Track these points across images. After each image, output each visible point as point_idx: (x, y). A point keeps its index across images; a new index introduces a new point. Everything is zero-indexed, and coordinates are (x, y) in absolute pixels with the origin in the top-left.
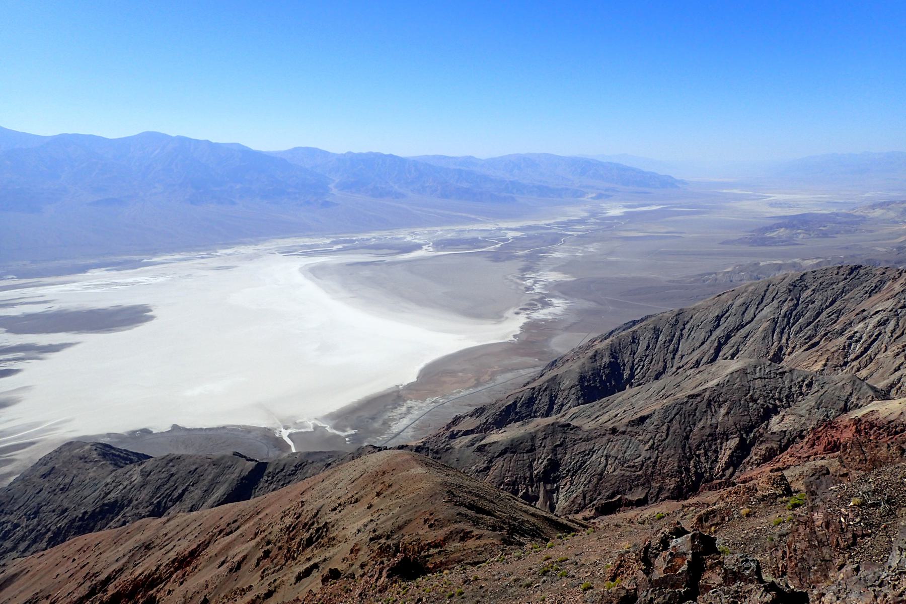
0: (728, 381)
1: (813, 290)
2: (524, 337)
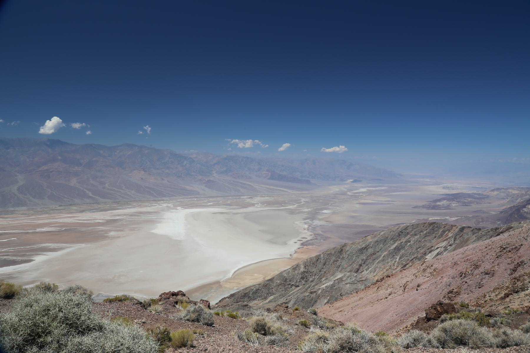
0: (332, 285)
1: (411, 235)
2: (295, 256)
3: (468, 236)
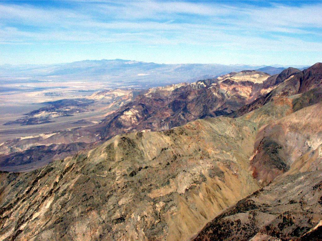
3: (3, 185)
